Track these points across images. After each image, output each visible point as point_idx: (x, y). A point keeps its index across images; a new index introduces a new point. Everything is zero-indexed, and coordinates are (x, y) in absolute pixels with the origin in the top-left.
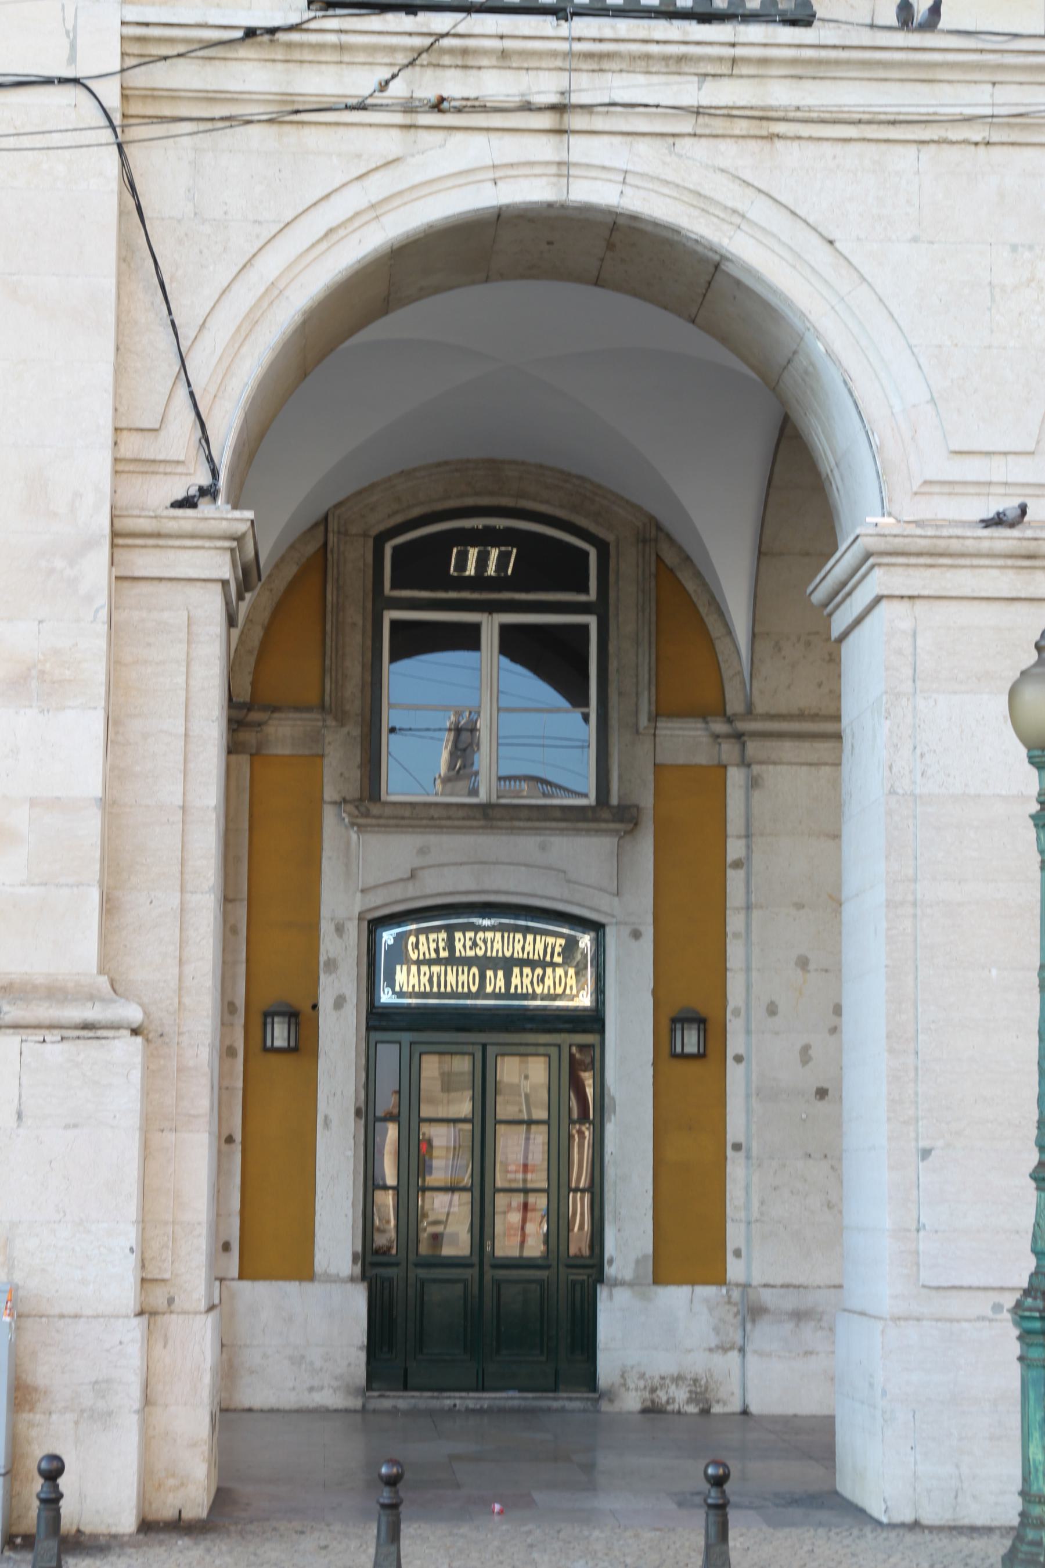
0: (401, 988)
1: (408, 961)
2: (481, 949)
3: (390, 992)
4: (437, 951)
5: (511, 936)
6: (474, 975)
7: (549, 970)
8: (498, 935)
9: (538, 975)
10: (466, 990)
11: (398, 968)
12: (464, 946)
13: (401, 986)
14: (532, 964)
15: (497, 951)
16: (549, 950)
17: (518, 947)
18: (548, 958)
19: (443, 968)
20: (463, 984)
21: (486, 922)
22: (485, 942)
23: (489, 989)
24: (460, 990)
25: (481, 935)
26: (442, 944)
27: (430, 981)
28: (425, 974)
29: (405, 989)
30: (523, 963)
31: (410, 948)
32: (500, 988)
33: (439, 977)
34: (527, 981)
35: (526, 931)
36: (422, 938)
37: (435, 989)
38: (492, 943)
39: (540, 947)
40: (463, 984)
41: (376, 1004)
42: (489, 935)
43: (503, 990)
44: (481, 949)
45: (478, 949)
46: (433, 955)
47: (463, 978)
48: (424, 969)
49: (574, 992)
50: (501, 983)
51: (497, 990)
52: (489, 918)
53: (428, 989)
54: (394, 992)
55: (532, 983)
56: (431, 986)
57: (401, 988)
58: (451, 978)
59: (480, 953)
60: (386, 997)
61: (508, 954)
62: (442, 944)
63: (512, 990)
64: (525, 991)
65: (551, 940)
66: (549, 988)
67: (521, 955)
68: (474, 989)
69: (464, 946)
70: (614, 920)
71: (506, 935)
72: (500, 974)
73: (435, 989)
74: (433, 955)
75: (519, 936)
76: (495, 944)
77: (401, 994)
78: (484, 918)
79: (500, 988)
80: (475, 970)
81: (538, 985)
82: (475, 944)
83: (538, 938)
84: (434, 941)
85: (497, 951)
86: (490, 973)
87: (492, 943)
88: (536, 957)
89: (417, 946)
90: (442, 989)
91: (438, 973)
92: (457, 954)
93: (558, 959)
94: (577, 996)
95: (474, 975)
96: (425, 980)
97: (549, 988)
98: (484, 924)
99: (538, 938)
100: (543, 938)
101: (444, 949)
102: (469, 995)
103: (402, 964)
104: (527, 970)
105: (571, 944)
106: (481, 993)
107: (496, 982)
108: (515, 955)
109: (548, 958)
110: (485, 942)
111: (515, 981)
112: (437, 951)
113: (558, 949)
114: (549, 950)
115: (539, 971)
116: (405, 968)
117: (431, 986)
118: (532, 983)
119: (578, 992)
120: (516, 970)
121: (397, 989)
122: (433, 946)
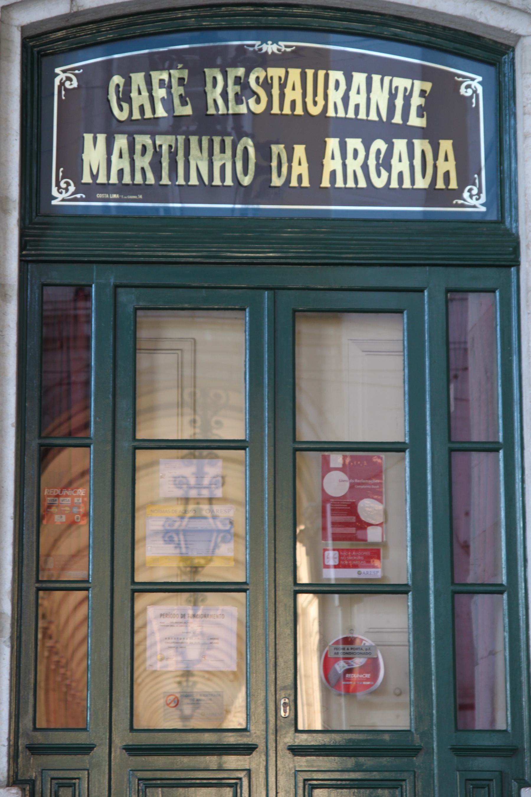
0: (94, 177)
2: (258, 101)
3: (72, 189)
5: (321, 74)
7: (400, 145)
8: (295, 74)
9: (379, 151)
11: (88, 138)
12: (224, 94)
13: (95, 172)
15: (293, 103)
16: (399, 102)
17: (335, 96)
18: (397, 119)
19: (181, 139)
21: (270, 48)
22: (267, 85)
23: (277, 181)
24: (217, 182)
25: (258, 73)
27: (156, 166)
28: (144, 147)
29: (102, 179)
32: (300, 177)
34: (354, 165)
36: (138, 79)
38: (282, 86)
41: (43, 211)
42: (275, 73)
43: (306, 183)
44: (258, 101)
45: (252, 102)
46: (161, 112)
49: (453, 185)
51: (294, 183)
52: (275, 42)
53: (151, 179)
54: (81, 187)
55: (365, 167)
56: (158, 176)
57: (94, 177)
59: (259, 109)
61: (315, 111)
62: (177, 91)
63: (326, 183)
64: (351, 184)
66: (401, 175)
67: (341, 114)
68: (246, 181)
71: (310, 73)
72: (300, 151)
75: (336, 75)
76: (288, 90)
79: (300, 177)
81: (379, 175)
83: (376, 78)
84: (162, 83)
85: (293, 103)
86: (277, 149)
88: (373, 117)
92: (211, 111)
93: (415, 121)
94: (458, 193)
97: (401, 175)
98: (264, 50)
99: (376, 78)
100: (387, 79)
101: (184, 103)
103: (95, 132)
104: (354, 143)
108: (331, 113)
109: (397, 119)
110: (267, 85)
112: (168, 103)
113: (416, 101)
114: (399, 102)
115: (379, 144)
116: (101, 138)
117: (158, 176)
118: (365, 167)
120: (332, 144)
121: (87, 179)
122: (160, 93)
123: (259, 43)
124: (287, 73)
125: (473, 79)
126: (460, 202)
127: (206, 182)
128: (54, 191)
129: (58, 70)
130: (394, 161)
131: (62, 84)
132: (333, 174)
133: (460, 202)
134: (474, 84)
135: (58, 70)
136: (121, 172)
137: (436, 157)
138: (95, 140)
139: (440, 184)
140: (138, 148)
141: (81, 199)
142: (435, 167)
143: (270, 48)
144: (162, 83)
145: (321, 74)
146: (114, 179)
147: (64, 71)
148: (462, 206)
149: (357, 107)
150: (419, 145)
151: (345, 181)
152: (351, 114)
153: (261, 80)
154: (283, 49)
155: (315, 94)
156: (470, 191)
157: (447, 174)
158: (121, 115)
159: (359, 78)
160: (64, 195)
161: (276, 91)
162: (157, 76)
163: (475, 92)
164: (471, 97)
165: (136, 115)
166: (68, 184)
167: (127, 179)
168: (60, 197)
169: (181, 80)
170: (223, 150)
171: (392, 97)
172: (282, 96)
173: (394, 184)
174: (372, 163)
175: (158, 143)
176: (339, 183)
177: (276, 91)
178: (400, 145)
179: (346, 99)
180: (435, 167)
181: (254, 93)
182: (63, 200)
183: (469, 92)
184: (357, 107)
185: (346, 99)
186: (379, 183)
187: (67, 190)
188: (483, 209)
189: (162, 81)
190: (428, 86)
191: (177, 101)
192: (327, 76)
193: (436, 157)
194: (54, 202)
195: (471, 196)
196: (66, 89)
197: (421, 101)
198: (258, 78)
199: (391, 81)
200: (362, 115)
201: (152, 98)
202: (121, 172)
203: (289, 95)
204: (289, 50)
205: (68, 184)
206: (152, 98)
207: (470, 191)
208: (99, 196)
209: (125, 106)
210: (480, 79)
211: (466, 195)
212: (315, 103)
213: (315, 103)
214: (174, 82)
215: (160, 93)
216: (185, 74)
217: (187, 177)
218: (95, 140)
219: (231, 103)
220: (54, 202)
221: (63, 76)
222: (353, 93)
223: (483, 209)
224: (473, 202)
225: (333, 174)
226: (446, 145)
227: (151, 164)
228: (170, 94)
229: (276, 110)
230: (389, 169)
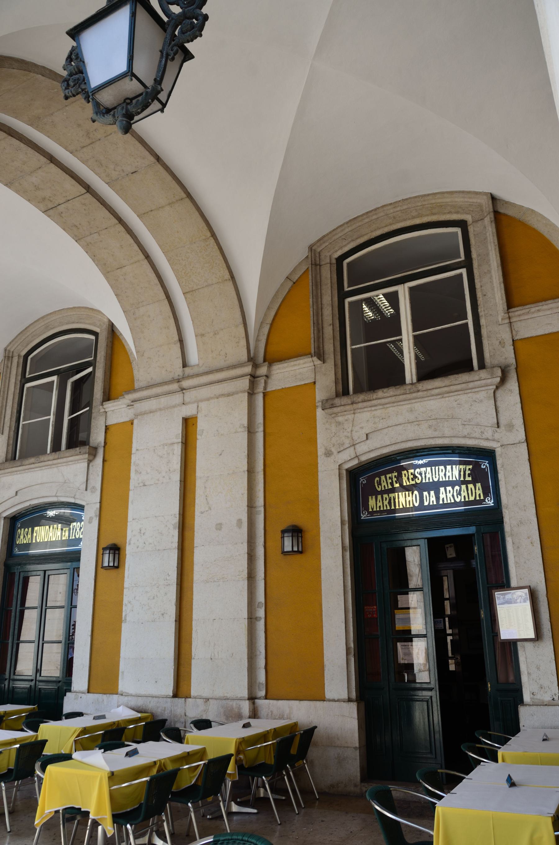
0: (372, 509)
1: (376, 493)
2: (418, 479)
3: (366, 513)
4: (392, 484)
6: (416, 495)
8: (429, 469)
10: (411, 506)
11: (370, 497)
12: (408, 479)
14: (452, 484)
15: (429, 478)
16: (462, 473)
17: (442, 474)
18: (462, 479)
20: (409, 501)
21: (421, 462)
22: (421, 474)
23: (426, 504)
24: (408, 506)
25: (418, 470)
26: (395, 479)
27: (390, 503)
28: (386, 498)
29: (375, 510)
30: (445, 484)
31: (376, 484)
32: (433, 501)
33: (394, 499)
34: (450, 495)
35: (445, 464)
37: (393, 508)
38: (425, 473)
39: (456, 473)
40: (409, 501)
42: (423, 470)
43: (435, 503)
45: (416, 479)
46: (390, 487)
47: (408, 499)
48: (385, 496)
49: (482, 498)
50: (433, 499)
51: (431, 504)
52: (422, 460)
53: (389, 508)
54: (369, 512)
55: (453, 496)
57: (372, 509)
58: (402, 500)
59: (418, 482)
60: (364, 516)
61: (436, 480)
63: (441, 502)
64: (449, 502)
65: (462, 467)
67: (444, 479)
68: (417, 505)
69: (408, 479)
70: (499, 445)
71: (433, 468)
72: (432, 493)
73: (393, 508)
74: (390, 487)
75: (442, 467)
76: (427, 475)
77: (372, 513)
78: (419, 460)
79: (433, 501)
80: (416, 492)
82: (415, 477)
83: (454, 466)
85: (429, 478)
86: (425, 493)
87: (425, 473)
88: (454, 479)
89: (380, 483)
90: (397, 507)
91: (394, 497)
92: (405, 484)
94: (484, 500)
95: (416, 495)
96: (386, 503)
97: (465, 497)
99: (454, 466)
100: (458, 466)
102: (415, 509)
103: (372, 495)
104: (449, 488)
105: (477, 466)
106: (422, 506)
107: (430, 498)
110: (421, 474)
111: (442, 496)
113: (468, 472)
115: (457, 488)
116: (374, 497)
117: (391, 506)
118: (453, 496)
119: (485, 498)
120: (442, 489)
121: (370, 510)
122: (390, 481)
123: (417, 461)
124: (426, 469)
125: (485, 462)
126: (485, 503)
127: (405, 507)
128: (362, 515)
129: (360, 479)
130: (462, 493)
131: (362, 482)
132: (443, 499)
133: (485, 503)
134: (486, 464)
135: (360, 479)
136: (380, 507)
137: (475, 489)
138: (372, 498)
139: (478, 498)
140: (384, 499)
141: (369, 516)
142: (476, 493)
143: (421, 462)
144: (390, 477)
145: (437, 468)
146: (378, 509)
147: (362, 479)
148: (486, 504)
149: (449, 477)
150: (471, 486)
151: (447, 501)
152: (447, 479)
153: (419, 473)
154: (425, 462)
155: (435, 474)
156: (488, 499)
157: (480, 495)
158: (379, 489)
159: (449, 467)
160: (364, 516)
161: (423, 476)
162: (388, 476)
163: (486, 466)
164: (485, 468)
165: (383, 489)
166: (365, 512)
167: (382, 509)
168: (364, 516)
169: (395, 476)
170: (409, 496)
171: (460, 471)
172: (425, 477)
173: (463, 500)
174: (455, 494)
175: (390, 497)
176: (445, 502)
177: (423, 476)
178: (464, 487)
179: (445, 475)
180: (476, 493)
181: (417, 477)
182: (364, 517)
183: (485, 467)
184: (449, 477)
185: (445, 475)
186: (458, 500)
187: (365, 514)
188: (493, 504)
189: (390, 477)
190: (471, 467)
191: (394, 483)
192: (439, 468)
193: (475, 489)
194: (362, 518)
195: (488, 501)
196: (363, 484)
197: (469, 472)
198: (418, 472)
199: (459, 467)
200: (451, 479)
201: (387, 483)
202: (380, 507)
203: (428, 476)
204: (426, 462)
205: (365, 512)
206: (387, 483)
207: (488, 499)
208: (374, 515)
209: (380, 486)
210: (487, 462)
211: (487, 500)
212: (436, 477)
213: (436, 477)
214: (393, 477)
215: (390, 481)
216: (396, 474)
217: (399, 506)
218: (372, 498)
219: (411, 481)
220: (362, 518)
221: (362, 480)
222: (447, 473)
223: (493, 504)
224: (489, 503)
225: (443, 499)
226: (479, 485)
227: (388, 503)
228: (392, 481)
229: (424, 481)
230: (460, 495)
